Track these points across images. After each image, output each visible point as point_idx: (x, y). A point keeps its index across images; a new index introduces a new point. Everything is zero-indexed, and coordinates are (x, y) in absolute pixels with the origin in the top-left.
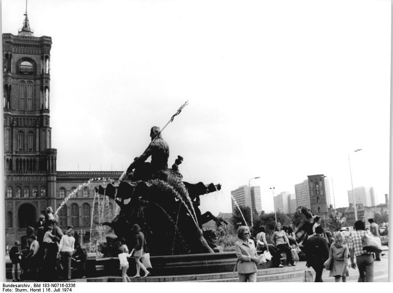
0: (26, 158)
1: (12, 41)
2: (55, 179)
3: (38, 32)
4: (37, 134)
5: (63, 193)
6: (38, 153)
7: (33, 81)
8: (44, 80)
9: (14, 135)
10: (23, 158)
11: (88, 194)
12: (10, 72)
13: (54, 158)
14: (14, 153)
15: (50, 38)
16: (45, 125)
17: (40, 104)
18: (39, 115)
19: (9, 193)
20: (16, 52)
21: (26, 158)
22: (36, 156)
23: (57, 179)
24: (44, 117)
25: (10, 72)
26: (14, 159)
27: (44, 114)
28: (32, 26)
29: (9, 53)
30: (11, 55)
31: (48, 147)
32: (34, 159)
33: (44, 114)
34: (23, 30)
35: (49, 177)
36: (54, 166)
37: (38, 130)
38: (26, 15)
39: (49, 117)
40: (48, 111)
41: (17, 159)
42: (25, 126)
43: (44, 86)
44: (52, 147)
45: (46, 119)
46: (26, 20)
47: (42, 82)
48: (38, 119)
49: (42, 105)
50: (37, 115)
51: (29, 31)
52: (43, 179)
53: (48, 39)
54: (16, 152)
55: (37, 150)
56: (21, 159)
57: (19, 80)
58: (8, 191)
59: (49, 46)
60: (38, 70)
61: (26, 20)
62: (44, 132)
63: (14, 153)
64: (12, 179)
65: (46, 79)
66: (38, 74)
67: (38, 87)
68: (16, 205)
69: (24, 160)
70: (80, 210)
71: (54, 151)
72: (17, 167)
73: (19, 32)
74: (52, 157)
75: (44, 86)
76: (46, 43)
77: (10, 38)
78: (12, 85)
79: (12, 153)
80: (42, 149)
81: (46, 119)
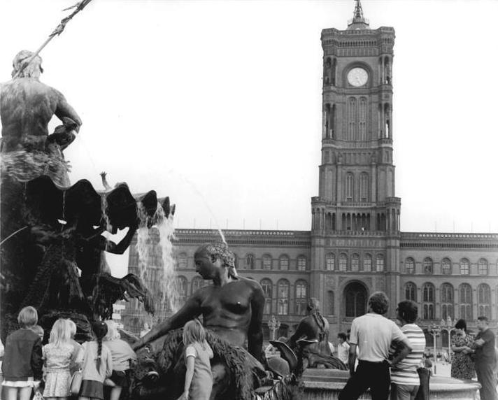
1: (336, 39)
2: (398, 244)
3: (374, 22)
4: (374, 176)
5: (466, 267)
6: (374, 205)
7: (367, 96)
8: (383, 94)
9: (339, 178)
11: (488, 270)
12: (334, 85)
13: (396, 211)
14: (339, 205)
15: (391, 29)
16: (384, 161)
18: (377, 147)
19: (380, 265)
20: (364, 54)
22: (372, 209)
23: (401, 245)
24: (384, 149)
25: (334, 85)
26: (339, 213)
27: (383, 145)
28: (367, 15)
29: (332, 57)
30: (335, 60)
31: (390, 195)
32: (369, 215)
33: (383, 145)
34: (354, 22)
35: (389, 241)
36: (396, 224)
37: (374, 170)
39: (392, 149)
40: (390, 140)
41: (344, 214)
42: (357, 165)
43: (383, 103)
44: (396, 196)
45: (387, 152)
47: (380, 96)
48: (374, 153)
50: (373, 147)
51: (362, 23)
52: (380, 243)
53: (388, 32)
54: (342, 204)
55: (374, 199)
56: (349, 214)
57: (348, 96)
58: (329, 261)
59: (391, 41)
60: (374, 80)
62: (383, 172)
63: (339, 205)
64: (334, 243)
65: (386, 93)
66: (375, 85)
67: (375, 106)
68: (340, 281)
69: (354, 214)
70: (475, 294)
71: (397, 202)
72: (343, 226)
73: (349, 26)
74: (393, 210)
76: (385, 36)
77: (333, 34)
78: (337, 104)
79: (336, 205)
80: (380, 199)
81: (387, 152)
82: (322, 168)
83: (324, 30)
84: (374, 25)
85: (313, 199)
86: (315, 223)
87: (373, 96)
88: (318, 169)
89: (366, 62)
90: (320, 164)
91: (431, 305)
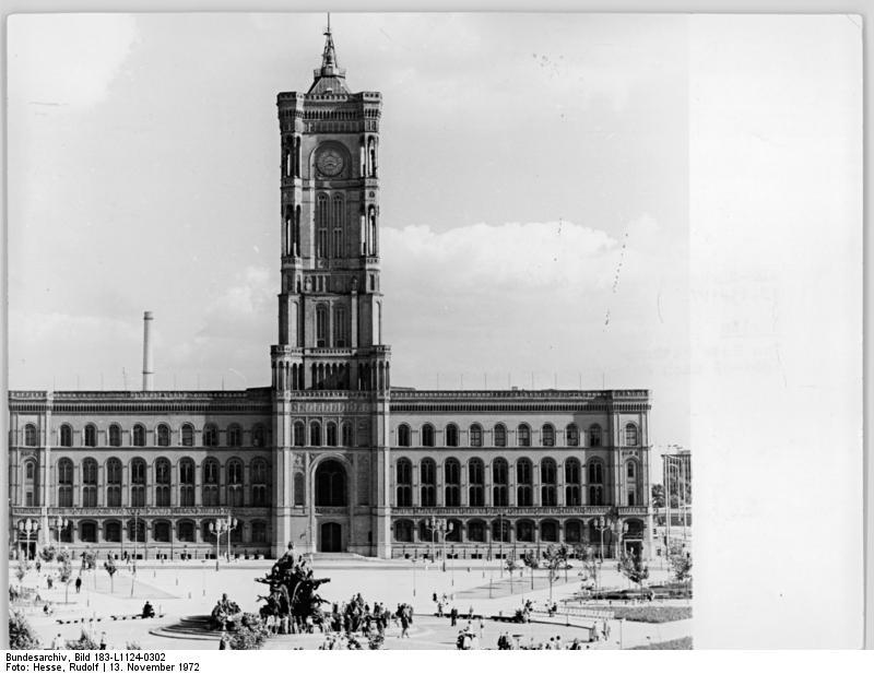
0: (331, 362)
2: (387, 409)
8: (367, 192)
10: (325, 362)
13: (385, 364)
14: (307, 352)
16: (368, 290)
17: (360, 243)
18: (358, 267)
21: (331, 362)
23: (393, 409)
24: (368, 273)
26: (309, 364)
28: (342, 62)
34: (322, 74)
37: (354, 301)
38: (328, 34)
41: (314, 365)
45: (372, 277)
46: (330, 46)
47: (363, 195)
49: (365, 244)
53: (373, 99)
54: (312, 350)
55: (354, 344)
56: (321, 365)
61: (330, 46)
63: (307, 352)
64: (301, 407)
65: (371, 190)
68: (312, 460)
75: (367, 204)
76: (367, 107)
79: (303, 352)
81: (372, 277)
82: (283, 299)
83: (281, 96)
84: (352, 86)
85: (273, 348)
86: (277, 379)
87: (353, 192)
88: (277, 299)
89: (343, 141)
90: (280, 292)
91: (503, 488)
